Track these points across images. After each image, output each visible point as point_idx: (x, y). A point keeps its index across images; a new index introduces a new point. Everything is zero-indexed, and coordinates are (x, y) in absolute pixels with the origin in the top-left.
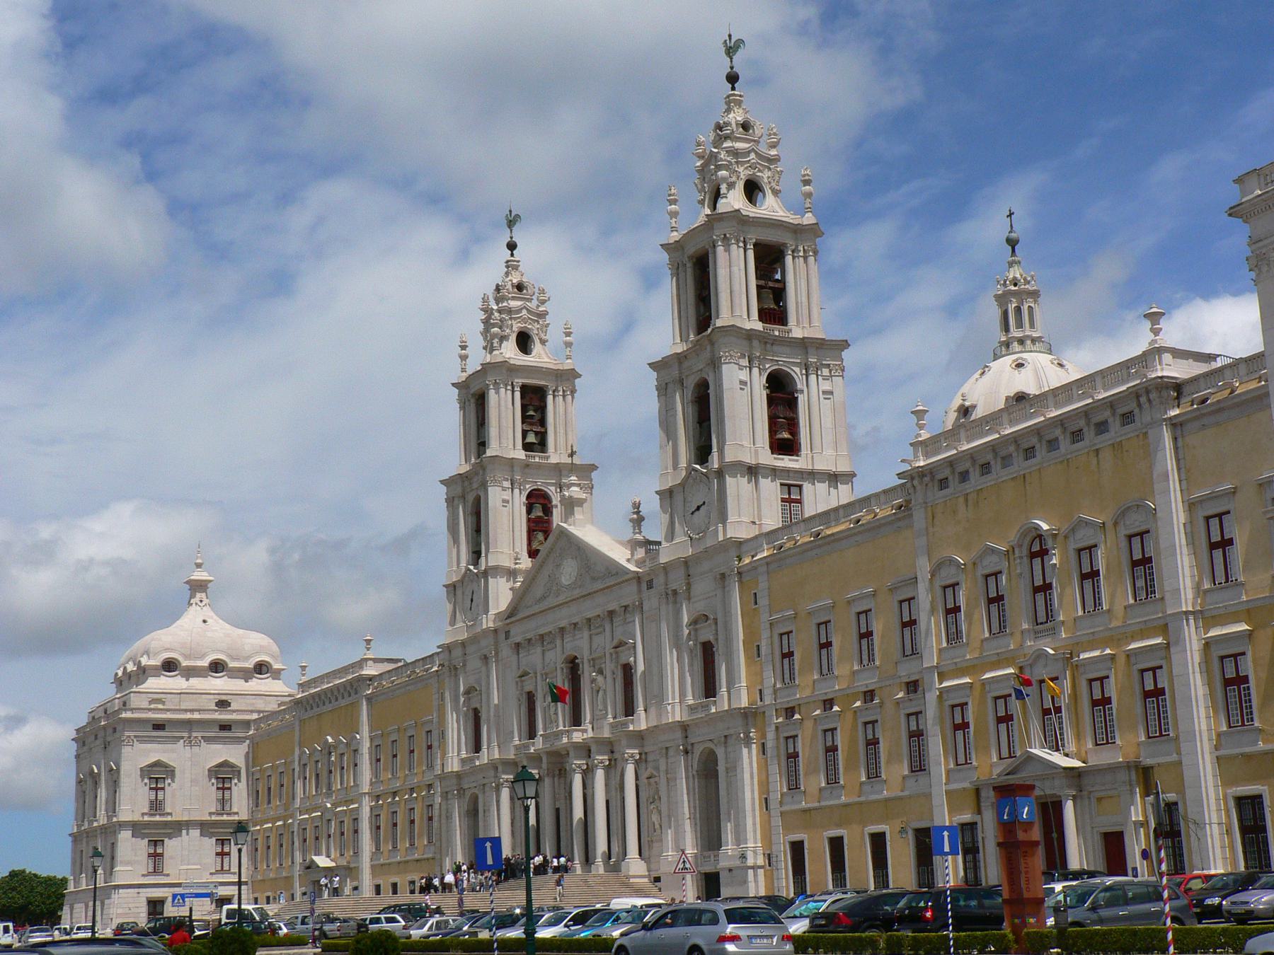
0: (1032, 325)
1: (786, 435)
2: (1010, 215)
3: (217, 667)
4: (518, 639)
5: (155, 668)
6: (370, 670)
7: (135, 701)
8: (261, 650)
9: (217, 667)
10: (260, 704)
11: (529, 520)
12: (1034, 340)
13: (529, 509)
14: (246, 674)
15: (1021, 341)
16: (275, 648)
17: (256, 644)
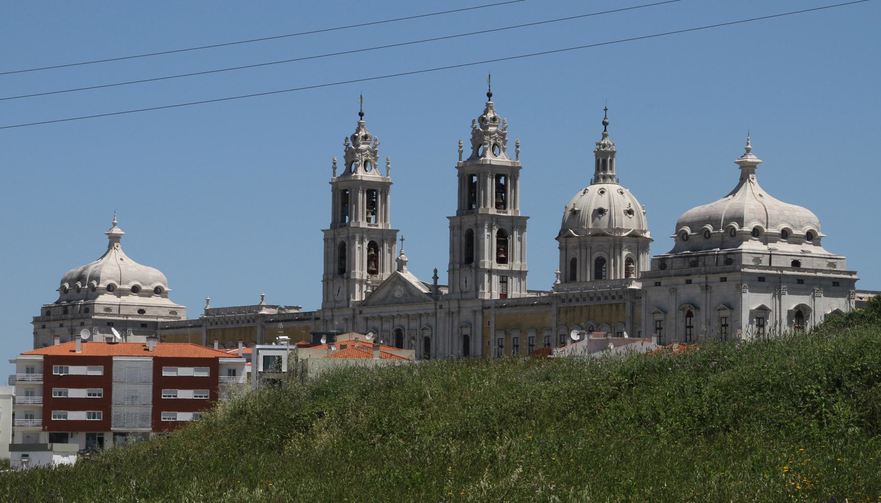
0: (611, 169)
1: (503, 256)
2: (606, 110)
3: (135, 290)
4: (368, 316)
5: (103, 289)
6: (265, 312)
7: (98, 309)
8: (158, 280)
9: (135, 290)
10: (161, 312)
11: (368, 256)
12: (611, 177)
13: (369, 250)
14: (148, 294)
15: (604, 178)
16: (164, 278)
17: (153, 276)
